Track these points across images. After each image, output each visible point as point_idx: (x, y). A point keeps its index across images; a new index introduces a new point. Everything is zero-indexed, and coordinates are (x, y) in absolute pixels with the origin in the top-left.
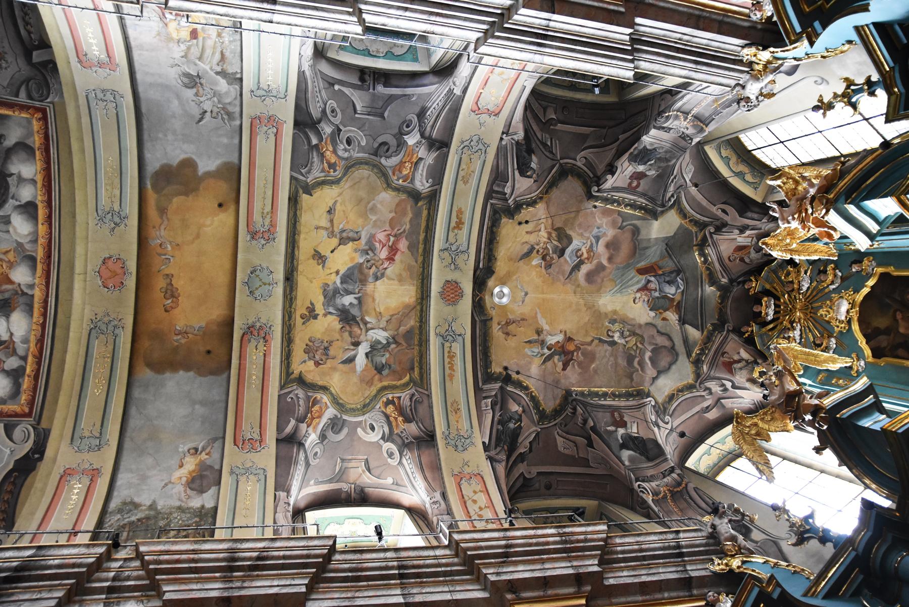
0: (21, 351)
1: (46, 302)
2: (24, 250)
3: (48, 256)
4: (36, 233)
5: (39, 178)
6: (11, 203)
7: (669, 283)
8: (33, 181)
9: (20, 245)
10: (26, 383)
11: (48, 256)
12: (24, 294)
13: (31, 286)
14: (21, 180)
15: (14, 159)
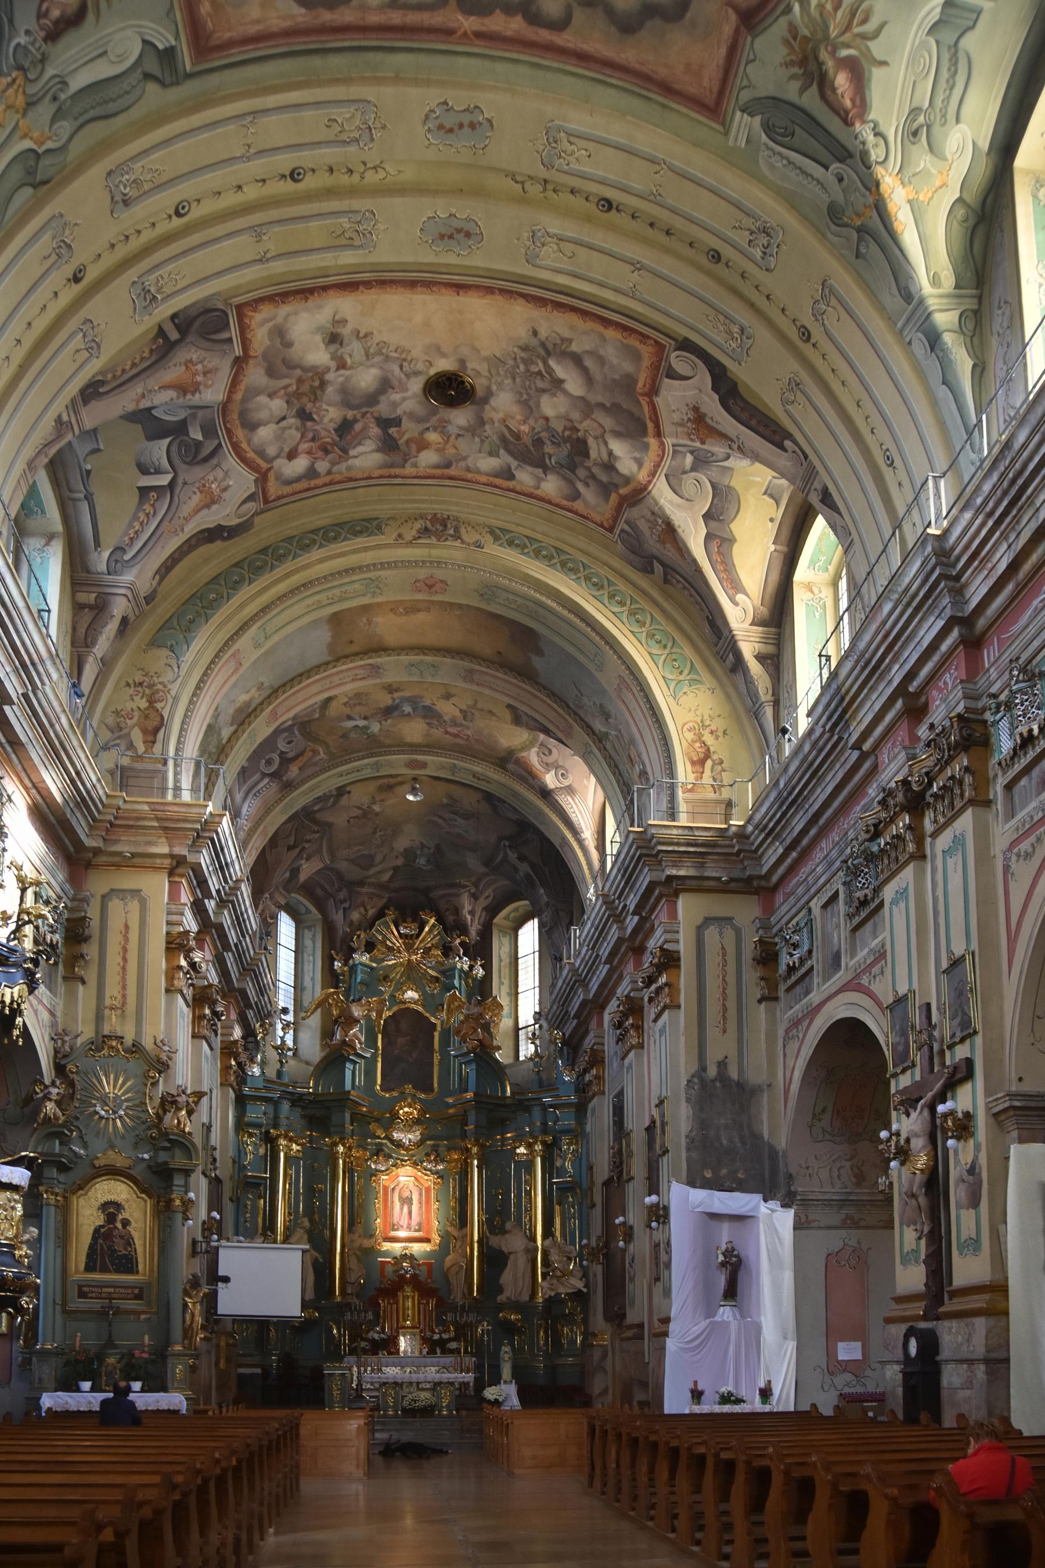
0: (335, 469)
1: (396, 477)
2: (458, 461)
3: (451, 478)
4: (478, 472)
5: (538, 492)
6: (514, 463)
7: (428, 861)
8: (538, 488)
9: (465, 458)
10: (303, 485)
11: (451, 478)
12: (406, 461)
13: (415, 465)
14: (539, 480)
15: (562, 483)
